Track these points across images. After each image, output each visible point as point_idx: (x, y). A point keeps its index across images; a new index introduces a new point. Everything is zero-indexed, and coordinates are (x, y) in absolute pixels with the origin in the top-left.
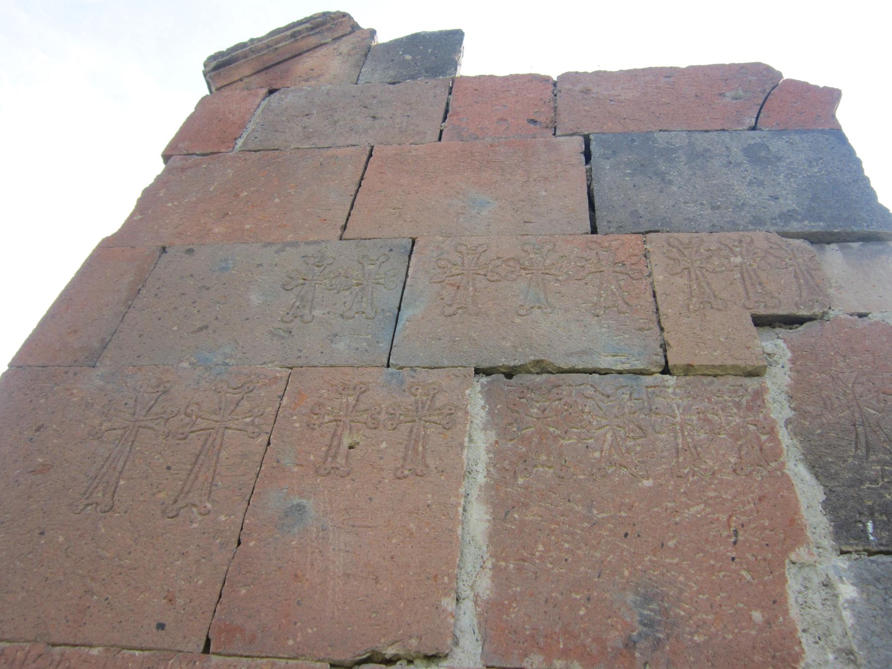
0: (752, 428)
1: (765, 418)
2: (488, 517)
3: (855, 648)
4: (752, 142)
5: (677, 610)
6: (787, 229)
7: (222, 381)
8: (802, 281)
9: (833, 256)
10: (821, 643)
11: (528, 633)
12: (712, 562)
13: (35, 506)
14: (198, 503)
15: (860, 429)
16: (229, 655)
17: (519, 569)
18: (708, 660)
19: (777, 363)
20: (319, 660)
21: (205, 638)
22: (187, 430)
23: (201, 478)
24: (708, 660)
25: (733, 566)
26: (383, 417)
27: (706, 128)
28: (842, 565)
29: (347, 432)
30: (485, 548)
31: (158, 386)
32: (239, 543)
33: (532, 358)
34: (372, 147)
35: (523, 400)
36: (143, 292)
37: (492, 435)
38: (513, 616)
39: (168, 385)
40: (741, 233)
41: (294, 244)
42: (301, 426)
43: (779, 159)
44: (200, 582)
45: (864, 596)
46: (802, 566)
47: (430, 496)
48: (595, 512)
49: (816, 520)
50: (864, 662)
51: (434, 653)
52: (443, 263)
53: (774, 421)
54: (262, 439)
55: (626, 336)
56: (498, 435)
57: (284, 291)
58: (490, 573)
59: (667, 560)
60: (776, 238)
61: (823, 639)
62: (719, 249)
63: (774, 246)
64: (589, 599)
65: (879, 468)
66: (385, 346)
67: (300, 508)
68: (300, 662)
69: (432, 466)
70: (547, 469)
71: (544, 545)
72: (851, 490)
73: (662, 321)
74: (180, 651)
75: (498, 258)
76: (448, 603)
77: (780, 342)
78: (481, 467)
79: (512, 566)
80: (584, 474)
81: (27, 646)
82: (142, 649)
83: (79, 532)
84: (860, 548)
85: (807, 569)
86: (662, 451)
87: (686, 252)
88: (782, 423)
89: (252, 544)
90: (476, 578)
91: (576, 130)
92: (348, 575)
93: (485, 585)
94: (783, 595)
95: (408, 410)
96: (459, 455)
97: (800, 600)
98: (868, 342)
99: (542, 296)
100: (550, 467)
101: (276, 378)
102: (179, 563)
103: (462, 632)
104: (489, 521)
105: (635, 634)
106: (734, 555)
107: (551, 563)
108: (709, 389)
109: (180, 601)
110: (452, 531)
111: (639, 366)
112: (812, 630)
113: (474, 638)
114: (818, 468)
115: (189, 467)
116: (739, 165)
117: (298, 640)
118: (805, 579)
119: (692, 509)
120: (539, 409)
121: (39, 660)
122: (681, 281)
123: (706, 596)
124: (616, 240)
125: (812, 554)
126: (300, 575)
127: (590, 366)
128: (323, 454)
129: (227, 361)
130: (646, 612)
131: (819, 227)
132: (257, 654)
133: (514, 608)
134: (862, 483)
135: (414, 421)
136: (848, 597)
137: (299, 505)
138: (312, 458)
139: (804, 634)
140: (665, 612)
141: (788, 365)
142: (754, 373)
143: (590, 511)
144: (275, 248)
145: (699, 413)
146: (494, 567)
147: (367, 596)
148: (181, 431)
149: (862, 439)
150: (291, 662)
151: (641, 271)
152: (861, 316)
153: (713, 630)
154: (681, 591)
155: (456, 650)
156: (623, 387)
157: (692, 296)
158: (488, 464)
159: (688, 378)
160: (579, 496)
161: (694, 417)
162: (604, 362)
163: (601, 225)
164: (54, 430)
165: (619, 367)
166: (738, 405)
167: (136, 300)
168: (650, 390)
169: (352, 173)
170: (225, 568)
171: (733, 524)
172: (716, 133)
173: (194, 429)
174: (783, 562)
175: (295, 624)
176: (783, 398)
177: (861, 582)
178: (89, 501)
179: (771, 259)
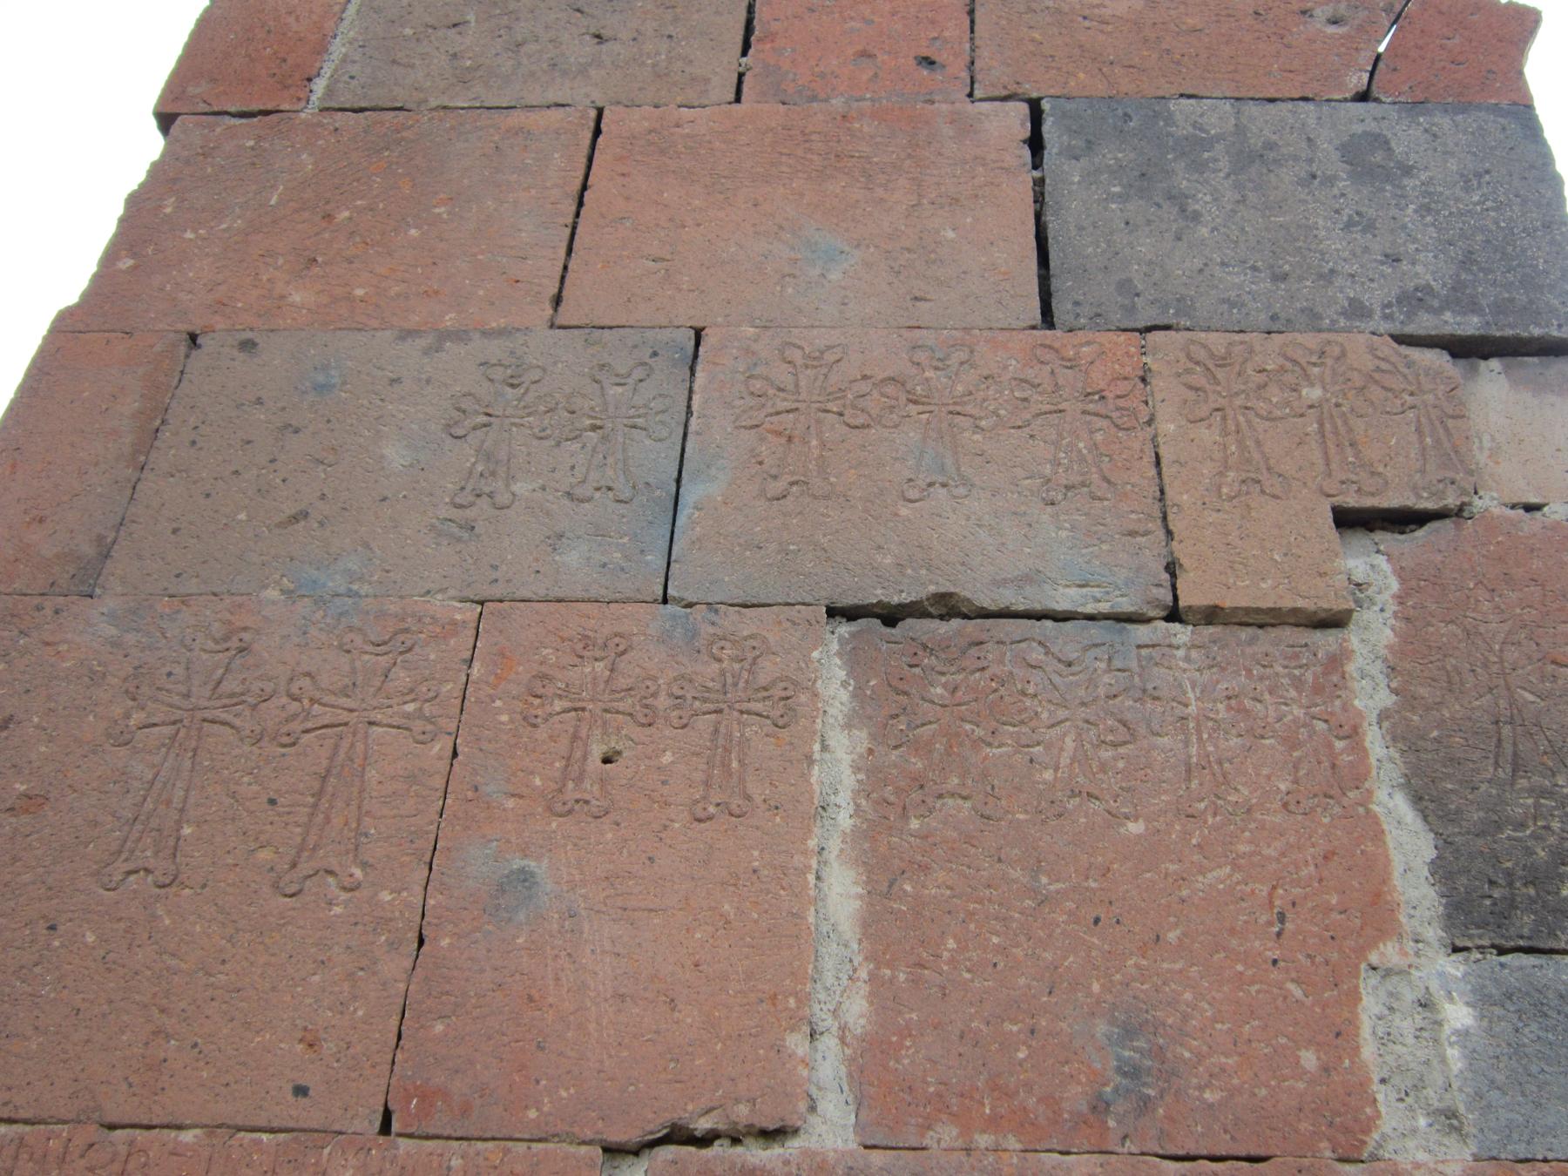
0: (1320, 726)
1: (1345, 708)
2: (860, 890)
3: (1462, 1109)
4: (1358, 129)
5: (1179, 1049)
6: (1410, 329)
7: (351, 629)
8: (1428, 440)
9: (1492, 386)
10: (1409, 1100)
11: (932, 1089)
12: (1240, 968)
13: (27, 878)
14: (337, 869)
15: (1506, 731)
16: (428, 1138)
17: (915, 981)
18: (1226, 1132)
19: (1372, 601)
20: (584, 1143)
21: (382, 1109)
22: (296, 726)
23: (337, 821)
24: (1226, 1132)
25: (1275, 975)
26: (662, 702)
27: (1272, 93)
28: (1453, 971)
29: (598, 732)
30: (855, 946)
31: (226, 638)
32: (421, 942)
33: (932, 589)
34: (600, 112)
35: (917, 670)
36: (166, 434)
37: (862, 736)
38: (906, 1061)
39: (247, 636)
40: (1325, 336)
41: (460, 336)
42: (512, 721)
43: (1408, 171)
44: (360, 1013)
45: (1485, 1023)
46: (1388, 973)
47: (756, 853)
48: (1044, 880)
49: (1415, 891)
50: (1474, 1131)
51: (777, 1126)
52: (757, 385)
53: (1360, 714)
54: (441, 746)
55: (1104, 547)
56: (873, 737)
57: (449, 440)
58: (865, 989)
59: (1165, 965)
60: (1388, 348)
61: (1412, 1094)
62: (1282, 370)
63: (1384, 366)
64: (1032, 1032)
65: (1530, 801)
66: (656, 560)
67: (525, 877)
68: (551, 1145)
69: (758, 799)
70: (960, 802)
71: (958, 941)
72: (1480, 842)
73: (1170, 517)
74: (341, 1133)
75: (865, 377)
76: (797, 1043)
77: (1381, 560)
78: (844, 798)
79: (902, 977)
80: (1026, 812)
81: (64, 1130)
82: (272, 1131)
83: (122, 925)
84: (1486, 942)
85: (1395, 979)
86: (1163, 770)
87: (1220, 374)
88: (1373, 718)
89: (445, 942)
90: (844, 999)
91: (1013, 88)
92: (622, 997)
93: (857, 1010)
94: (1353, 1022)
95: (708, 690)
96: (805, 777)
97: (1380, 1031)
98: (1536, 564)
99: (949, 462)
100: (965, 798)
101: (454, 623)
102: (316, 978)
103: (820, 1089)
104: (860, 897)
105: (1108, 1089)
106: (1276, 954)
107: (969, 971)
108: (1249, 650)
109: (329, 1047)
110: (799, 916)
111: (1126, 605)
112: (1396, 1080)
113: (842, 1098)
115: (311, 800)
116: (1330, 180)
117: (546, 1109)
118: (1391, 994)
119: (1209, 876)
120: (944, 686)
121: (91, 1153)
122: (1207, 435)
123: (1227, 1026)
124: (1088, 343)
125: (1406, 954)
126: (536, 996)
127: (1038, 607)
128: (557, 774)
129: (355, 587)
130: (1127, 1053)
132: (476, 1134)
133: (908, 1048)
134: (1499, 827)
135: (719, 711)
136: (1459, 1026)
137: (522, 870)
138: (538, 782)
139: (1382, 1087)
140: (1159, 1053)
141: (1392, 607)
142: (1334, 621)
143: (1035, 878)
144: (421, 343)
145: (1229, 698)
146: (873, 978)
147: (657, 1032)
148: (285, 730)
149: (1508, 748)
150: (536, 1146)
151: (1134, 414)
152: (1530, 508)
153: (1236, 1081)
154: (1185, 1018)
155: (812, 1119)
156: (1096, 645)
157: (1227, 467)
158: (856, 793)
159: (1211, 629)
160: (1016, 851)
161: (1220, 706)
162: (1064, 599)
163: (1060, 308)
164: (37, 727)
165: (1090, 609)
166: (1298, 683)
167: (154, 454)
168: (1144, 652)
169: (564, 168)
170: (402, 986)
171: (1278, 903)
172: (1290, 105)
173: (309, 725)
174: (1357, 966)
175: (538, 1082)
176: (1377, 669)
177: (1482, 1000)
178: (131, 866)
179: (1376, 393)
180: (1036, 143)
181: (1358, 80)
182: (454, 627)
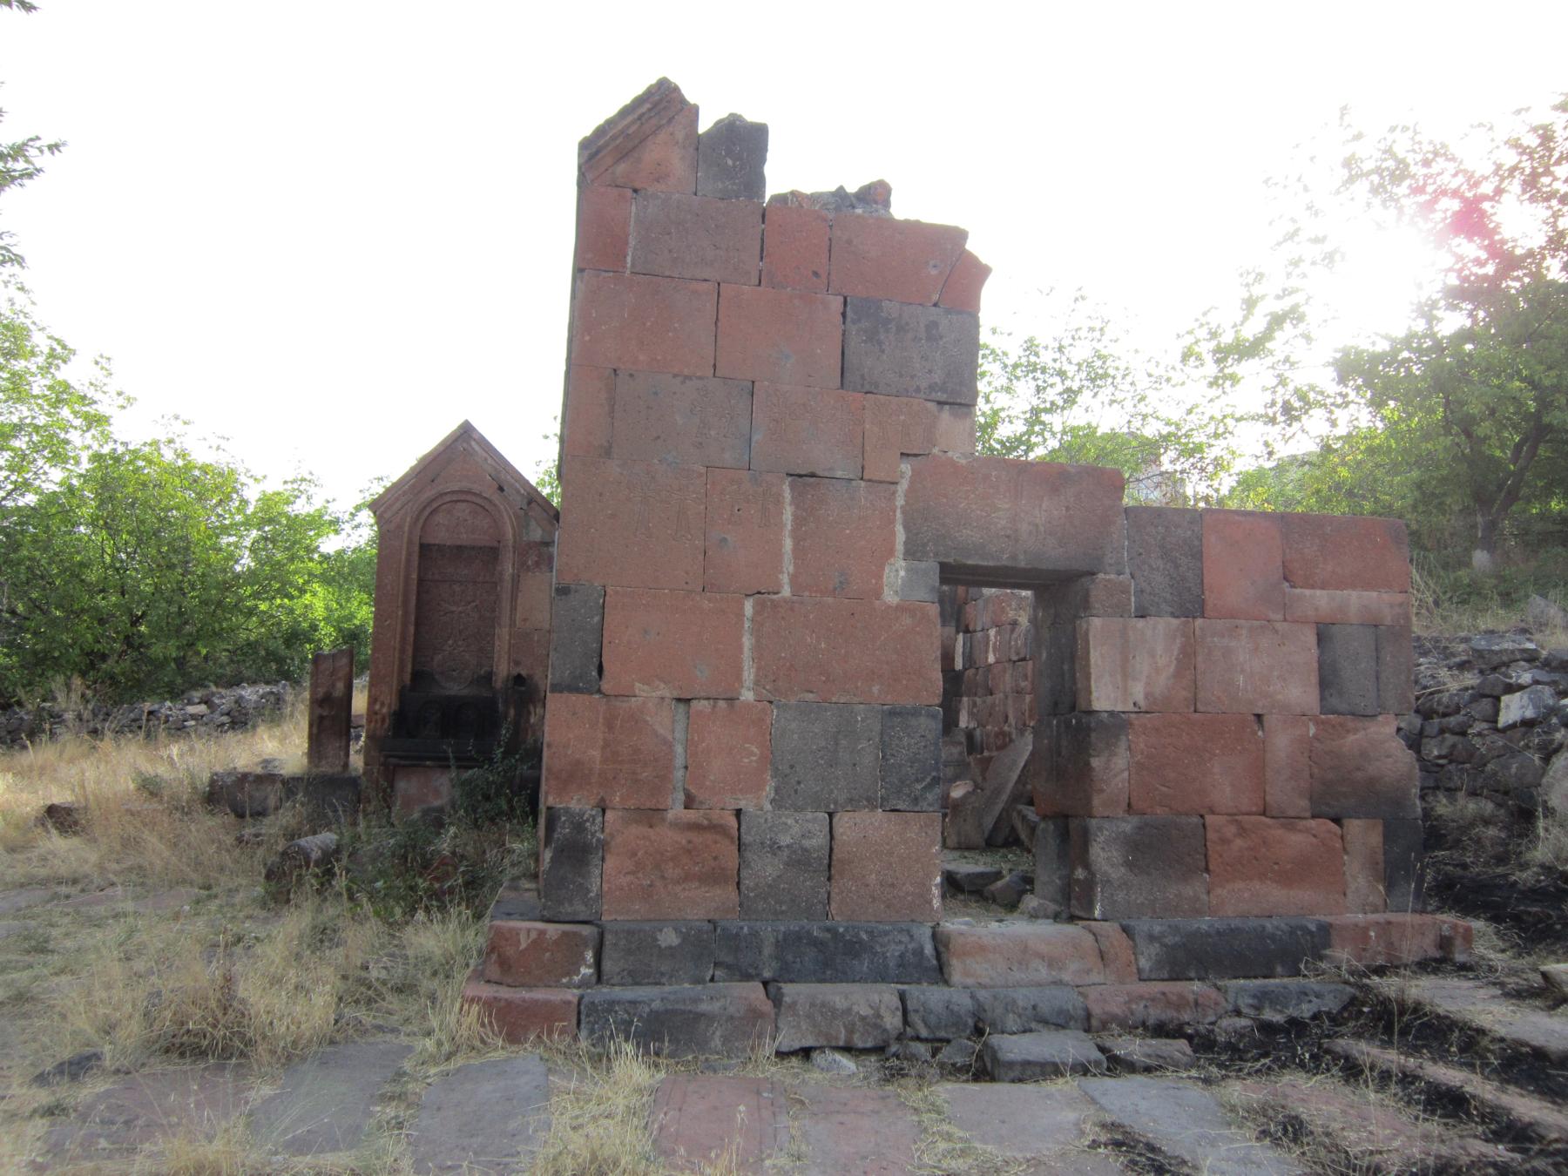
67: (725, 540)
90: (788, 566)
93: (791, 569)
114: (906, 528)
131: (942, 397)
162: (839, 474)
177: (907, 570)
180: (844, 315)
181: (935, 297)
182: (701, 475)
